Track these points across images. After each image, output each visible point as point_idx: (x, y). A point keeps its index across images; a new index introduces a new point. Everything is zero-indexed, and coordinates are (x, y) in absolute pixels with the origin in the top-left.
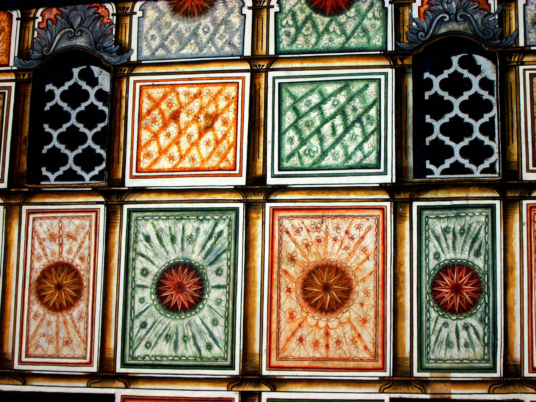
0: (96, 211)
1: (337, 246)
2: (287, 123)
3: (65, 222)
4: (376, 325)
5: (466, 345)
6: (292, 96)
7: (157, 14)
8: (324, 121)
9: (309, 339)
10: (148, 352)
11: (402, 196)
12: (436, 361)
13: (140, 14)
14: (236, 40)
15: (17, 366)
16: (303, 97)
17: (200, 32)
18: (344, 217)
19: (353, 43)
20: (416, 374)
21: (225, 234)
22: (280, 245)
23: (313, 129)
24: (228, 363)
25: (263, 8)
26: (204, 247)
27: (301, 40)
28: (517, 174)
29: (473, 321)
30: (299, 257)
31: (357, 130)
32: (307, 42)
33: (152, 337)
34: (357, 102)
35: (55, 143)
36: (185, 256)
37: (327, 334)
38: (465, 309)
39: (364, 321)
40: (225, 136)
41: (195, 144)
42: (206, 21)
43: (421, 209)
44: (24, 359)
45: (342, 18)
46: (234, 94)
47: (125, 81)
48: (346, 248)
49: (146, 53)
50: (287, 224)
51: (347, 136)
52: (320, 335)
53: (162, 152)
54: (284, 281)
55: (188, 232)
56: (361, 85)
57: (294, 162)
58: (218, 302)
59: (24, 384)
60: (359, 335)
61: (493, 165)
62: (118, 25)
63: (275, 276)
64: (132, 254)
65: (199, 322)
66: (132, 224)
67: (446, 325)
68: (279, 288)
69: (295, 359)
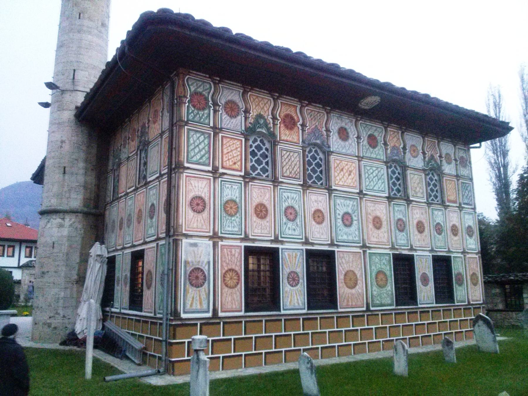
8: (374, 177)
14: (354, 150)
19: (378, 157)
20: (396, 247)
27: (367, 154)
28: (408, 198)
31: (380, 181)
33: (342, 234)
35: (309, 171)
41: (347, 178)
42: (347, 143)
45: (375, 150)
49: (334, 149)
53: (340, 179)
57: (368, 188)
58: (356, 224)
62: (327, 139)
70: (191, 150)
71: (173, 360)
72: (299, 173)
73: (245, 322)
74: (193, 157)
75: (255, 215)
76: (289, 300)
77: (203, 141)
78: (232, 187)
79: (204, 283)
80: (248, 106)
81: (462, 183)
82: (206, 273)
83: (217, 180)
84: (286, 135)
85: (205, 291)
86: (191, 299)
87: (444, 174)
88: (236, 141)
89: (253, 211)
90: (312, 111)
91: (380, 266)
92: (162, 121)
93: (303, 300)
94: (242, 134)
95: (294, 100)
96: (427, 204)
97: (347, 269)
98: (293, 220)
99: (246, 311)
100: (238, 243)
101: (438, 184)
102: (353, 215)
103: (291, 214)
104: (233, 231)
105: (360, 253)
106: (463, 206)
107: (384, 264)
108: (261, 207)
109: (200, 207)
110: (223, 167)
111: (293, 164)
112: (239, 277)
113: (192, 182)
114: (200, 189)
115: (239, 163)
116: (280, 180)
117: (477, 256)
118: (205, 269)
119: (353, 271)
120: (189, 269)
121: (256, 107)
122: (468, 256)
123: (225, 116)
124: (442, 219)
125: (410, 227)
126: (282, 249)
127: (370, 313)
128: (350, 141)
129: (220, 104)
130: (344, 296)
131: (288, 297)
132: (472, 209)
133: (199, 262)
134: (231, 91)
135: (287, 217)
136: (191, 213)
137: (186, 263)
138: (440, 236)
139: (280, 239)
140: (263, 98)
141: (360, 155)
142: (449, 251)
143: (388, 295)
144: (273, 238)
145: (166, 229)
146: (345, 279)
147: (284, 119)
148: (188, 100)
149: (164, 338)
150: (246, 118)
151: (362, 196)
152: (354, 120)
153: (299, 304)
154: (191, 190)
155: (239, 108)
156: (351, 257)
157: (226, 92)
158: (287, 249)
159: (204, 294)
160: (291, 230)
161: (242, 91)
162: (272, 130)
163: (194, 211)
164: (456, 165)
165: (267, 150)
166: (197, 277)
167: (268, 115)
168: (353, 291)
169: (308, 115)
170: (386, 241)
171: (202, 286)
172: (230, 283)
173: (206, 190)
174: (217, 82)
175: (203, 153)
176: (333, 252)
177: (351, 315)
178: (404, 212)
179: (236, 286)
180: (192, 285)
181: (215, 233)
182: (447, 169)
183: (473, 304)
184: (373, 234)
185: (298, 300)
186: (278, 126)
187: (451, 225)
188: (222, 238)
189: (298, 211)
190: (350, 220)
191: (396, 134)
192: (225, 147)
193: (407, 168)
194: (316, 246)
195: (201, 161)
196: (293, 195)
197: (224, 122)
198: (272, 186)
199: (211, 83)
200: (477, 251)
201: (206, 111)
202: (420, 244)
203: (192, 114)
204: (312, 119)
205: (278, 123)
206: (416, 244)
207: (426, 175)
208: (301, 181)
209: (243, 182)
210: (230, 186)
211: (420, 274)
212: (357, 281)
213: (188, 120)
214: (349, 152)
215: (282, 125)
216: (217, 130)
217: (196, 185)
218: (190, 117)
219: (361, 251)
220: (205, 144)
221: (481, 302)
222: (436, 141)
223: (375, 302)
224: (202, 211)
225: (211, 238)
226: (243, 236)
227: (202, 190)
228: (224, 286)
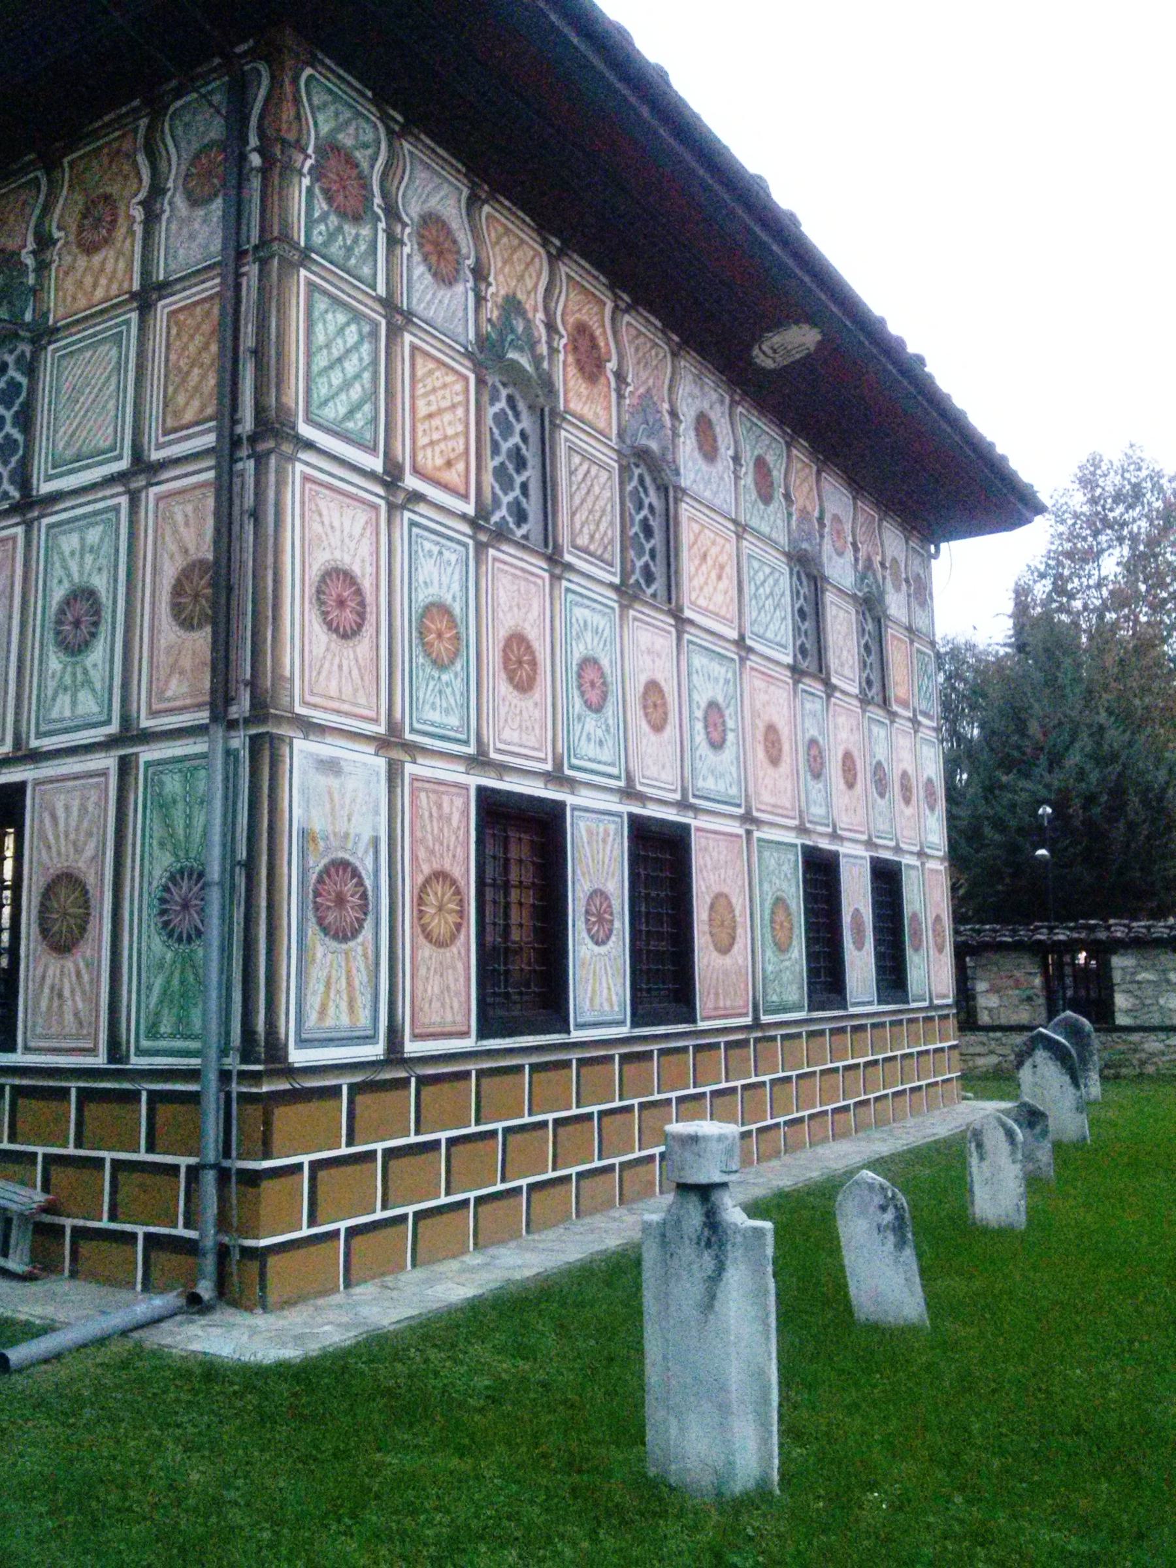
19: (774, 535)
70: (320, 374)
71: (263, 1243)
74: (325, 403)
75: (503, 676)
78: (440, 553)
79: (361, 926)
80: (484, 255)
85: (365, 955)
86: (322, 989)
92: (148, 235)
93: (621, 992)
94: (469, 355)
95: (597, 278)
96: (861, 701)
97: (716, 889)
102: (727, 713)
104: (444, 727)
114: (347, 540)
115: (461, 466)
118: (365, 866)
120: (317, 864)
121: (505, 263)
126: (574, 809)
127: (760, 1034)
129: (406, 219)
133: (346, 836)
134: (437, 180)
137: (307, 835)
145: (213, 691)
149: (211, 1157)
153: (612, 1006)
155: (458, 252)
158: (586, 810)
159: (362, 968)
160: (593, 744)
162: (545, 365)
164: (909, 595)
165: (524, 436)
166: (341, 898)
167: (535, 310)
168: (727, 961)
170: (788, 805)
173: (366, 549)
174: (397, 128)
175: (356, 392)
176: (686, 828)
180: (325, 930)
194: (651, 805)
195: (350, 425)
199: (379, 125)
201: (365, 231)
203: (322, 227)
206: (844, 821)
210: (436, 549)
217: (336, 524)
218: (318, 240)
219: (741, 831)
220: (361, 359)
221: (950, 1001)
225: (383, 744)
228: (421, 939)
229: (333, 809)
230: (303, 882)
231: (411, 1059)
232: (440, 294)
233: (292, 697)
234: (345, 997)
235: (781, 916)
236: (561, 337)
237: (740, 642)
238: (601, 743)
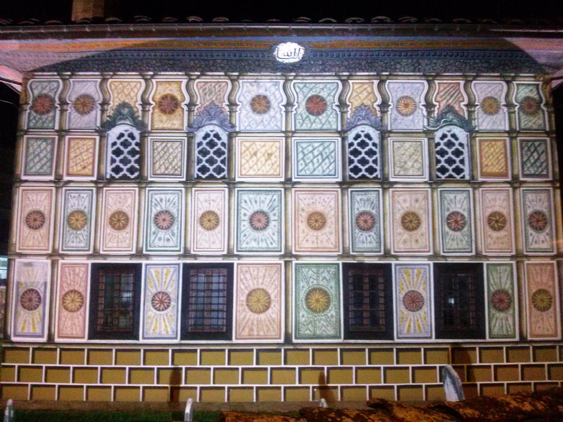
0: (223, 190)
1: (320, 205)
2: (299, 158)
3: (211, 195)
4: (336, 235)
5: (370, 242)
6: (302, 147)
7: (246, 112)
8: (315, 157)
9: (310, 241)
10: (247, 246)
11: (344, 186)
12: (359, 248)
13: (239, 112)
14: (279, 124)
15: (192, 253)
16: (306, 148)
17: (264, 120)
18: (322, 194)
19: (325, 127)
20: (351, 253)
21: (277, 200)
22: (298, 204)
23: (310, 160)
24: (279, 250)
25: (289, 112)
26: (268, 205)
27: (304, 125)
29: (372, 233)
30: (306, 209)
31: (327, 161)
32: (307, 126)
33: (248, 240)
34: (327, 150)
36: (261, 208)
37: (317, 238)
38: (369, 229)
39: (331, 233)
40: (276, 162)
41: (264, 165)
42: (266, 116)
43: (352, 191)
44: (195, 250)
45: (320, 117)
46: (278, 146)
47: (234, 139)
48: (324, 206)
50: (301, 196)
51: (323, 163)
52: (314, 239)
54: (300, 218)
55: (262, 200)
56: (328, 144)
57: (303, 173)
58: (275, 226)
59: (196, 259)
60: (329, 239)
61: (377, 175)
62: (230, 116)
63: (297, 216)
64: (239, 208)
65: (267, 234)
66: (239, 196)
67: (362, 235)
68: (298, 221)
69: (305, 248)
70: (31, 160)
72: (181, 167)
73: (89, 350)
74: (31, 168)
75: (109, 226)
76: (153, 327)
77: (45, 148)
78: (79, 196)
79: (38, 306)
80: (107, 97)
81: (522, 141)
82: (42, 295)
83: (60, 190)
84: (161, 121)
87: (477, 132)
88: (87, 141)
89: (107, 221)
90: (207, 82)
91: (315, 282)
93: (174, 327)
94: (96, 131)
95: (178, 75)
96: (430, 184)
97: (253, 287)
98: (168, 228)
99: (90, 338)
100: (84, 260)
101: (465, 151)
103: (164, 220)
105: (280, 264)
106: (522, 179)
107: (325, 278)
108: (118, 216)
109: (38, 223)
110: (68, 175)
111: (171, 157)
112: (82, 299)
113: (30, 196)
114: (39, 202)
115: (90, 167)
116: (150, 179)
117: (554, 262)
118: (41, 290)
119: (263, 289)
120: (22, 290)
122: (526, 262)
123: (75, 115)
124: (465, 206)
125: (387, 223)
126: (147, 265)
127: (292, 347)
128: (272, 112)
129: (69, 102)
130: (244, 323)
131: (152, 323)
132: (546, 182)
133: (34, 282)
134: (85, 84)
135: (157, 225)
136: (26, 230)
137: (19, 283)
138: (458, 233)
139: (144, 252)
140: (129, 82)
141: (289, 129)
142: (478, 255)
143: (329, 322)
144: (134, 252)
146: (247, 300)
147: (160, 102)
148: (29, 106)
150: (103, 111)
151: (290, 186)
152: (282, 82)
153: (167, 332)
154: (28, 205)
155: (94, 101)
156: (262, 269)
157: (78, 86)
159: (38, 317)
161: (99, 80)
162: (140, 119)
163: (30, 227)
164: (510, 113)
167: (136, 101)
168: (262, 316)
169: (198, 90)
171: (35, 308)
172: (71, 306)
173: (46, 203)
174: (67, 77)
177: (255, 348)
178: (375, 202)
179: (78, 309)
180: (24, 307)
181: (54, 250)
182: (485, 124)
183: (531, 342)
184: (308, 238)
185: (166, 326)
186: (150, 112)
187: (488, 213)
188: (63, 256)
189: (176, 215)
190: (264, 220)
191: (366, 86)
192: (72, 150)
193: (387, 135)
196: (168, 197)
197: (73, 120)
198: (137, 189)
200: (555, 253)
201: (51, 114)
202: (408, 246)
204: (205, 94)
205: (151, 109)
207: (429, 139)
208: (183, 178)
209: (94, 189)
211: (403, 293)
212: (269, 303)
213: (28, 129)
214: (268, 128)
215: (157, 110)
216: (62, 132)
217: (35, 198)
218: (31, 125)
219: (282, 262)
220: (47, 151)
222: (462, 83)
223: (302, 332)
224: (40, 227)
225: (49, 256)
226: (91, 252)
227: (40, 203)
228: (64, 310)
229: (29, 275)
230: (17, 295)
231: (57, 343)
232: (84, 117)
233: (15, 248)
234: (31, 325)
235: (317, 296)
236: (151, 104)
237: (288, 183)
238: (168, 240)
